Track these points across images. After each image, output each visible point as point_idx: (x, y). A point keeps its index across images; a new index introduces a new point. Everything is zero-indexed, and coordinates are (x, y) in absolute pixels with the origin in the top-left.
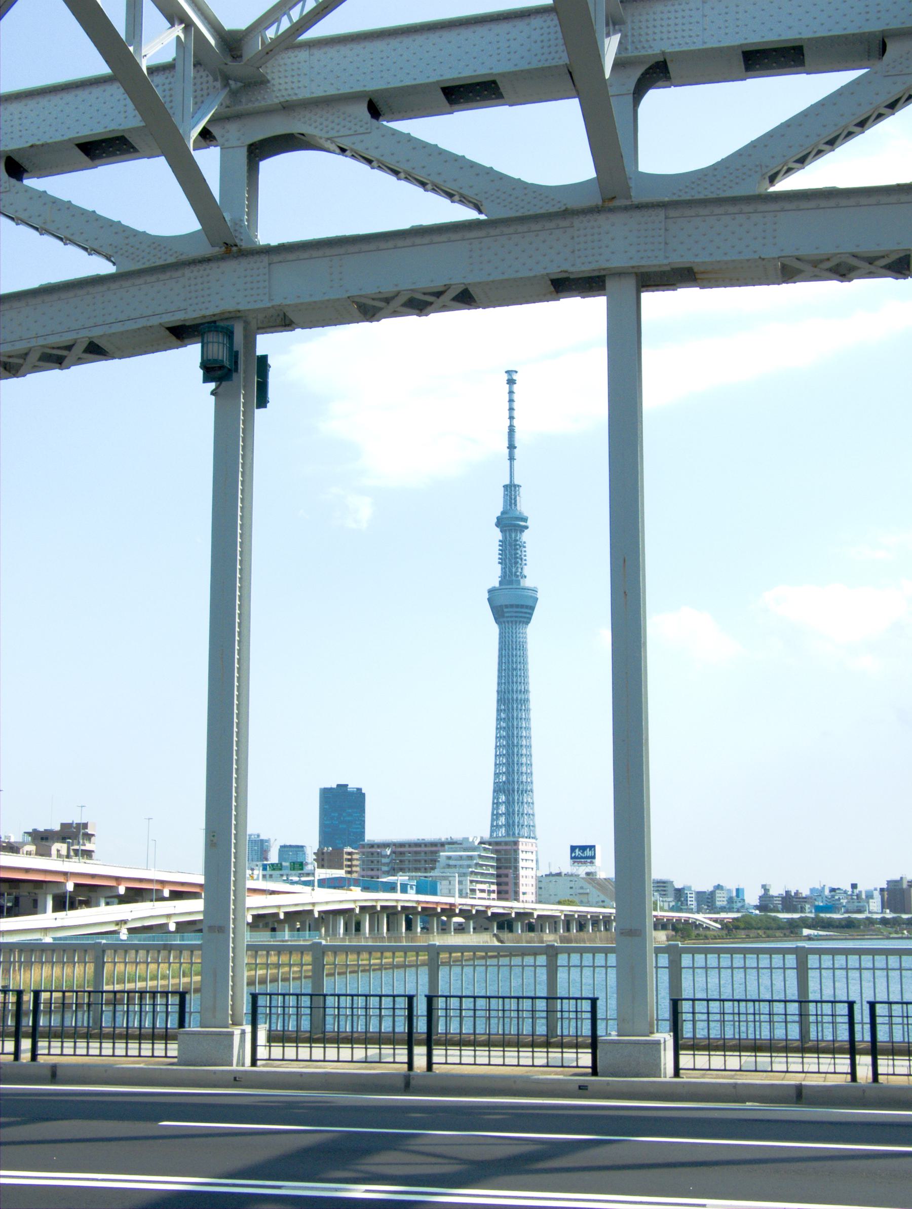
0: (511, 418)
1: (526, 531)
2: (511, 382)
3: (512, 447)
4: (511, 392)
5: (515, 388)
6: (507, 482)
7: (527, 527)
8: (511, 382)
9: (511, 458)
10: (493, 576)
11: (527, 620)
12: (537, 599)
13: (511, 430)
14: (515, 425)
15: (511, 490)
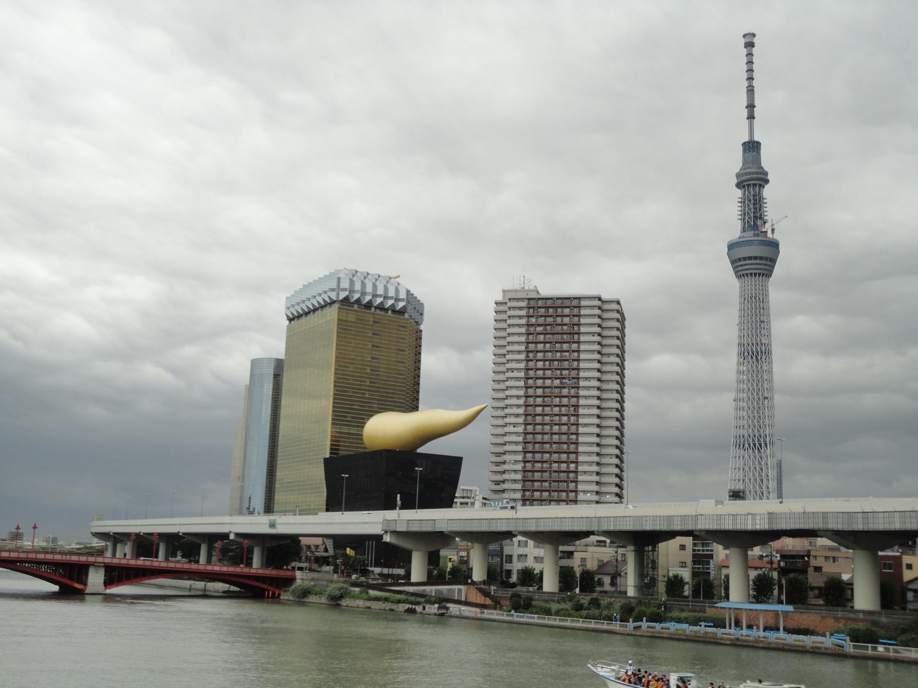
0: (750, 79)
1: (766, 186)
2: (750, 45)
3: (751, 107)
4: (750, 55)
5: (754, 51)
6: (747, 139)
7: (767, 181)
8: (750, 45)
9: (751, 117)
10: (734, 231)
11: (768, 273)
12: (779, 252)
13: (751, 90)
14: (754, 85)
15: (752, 147)
